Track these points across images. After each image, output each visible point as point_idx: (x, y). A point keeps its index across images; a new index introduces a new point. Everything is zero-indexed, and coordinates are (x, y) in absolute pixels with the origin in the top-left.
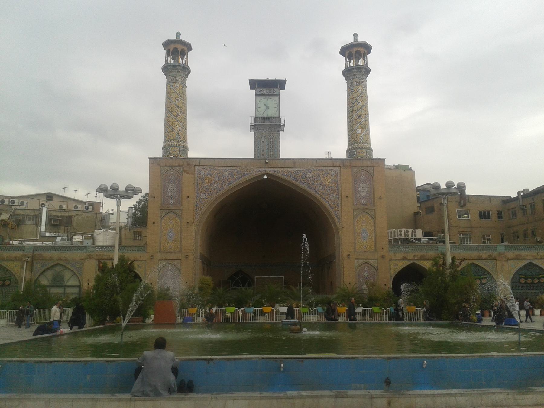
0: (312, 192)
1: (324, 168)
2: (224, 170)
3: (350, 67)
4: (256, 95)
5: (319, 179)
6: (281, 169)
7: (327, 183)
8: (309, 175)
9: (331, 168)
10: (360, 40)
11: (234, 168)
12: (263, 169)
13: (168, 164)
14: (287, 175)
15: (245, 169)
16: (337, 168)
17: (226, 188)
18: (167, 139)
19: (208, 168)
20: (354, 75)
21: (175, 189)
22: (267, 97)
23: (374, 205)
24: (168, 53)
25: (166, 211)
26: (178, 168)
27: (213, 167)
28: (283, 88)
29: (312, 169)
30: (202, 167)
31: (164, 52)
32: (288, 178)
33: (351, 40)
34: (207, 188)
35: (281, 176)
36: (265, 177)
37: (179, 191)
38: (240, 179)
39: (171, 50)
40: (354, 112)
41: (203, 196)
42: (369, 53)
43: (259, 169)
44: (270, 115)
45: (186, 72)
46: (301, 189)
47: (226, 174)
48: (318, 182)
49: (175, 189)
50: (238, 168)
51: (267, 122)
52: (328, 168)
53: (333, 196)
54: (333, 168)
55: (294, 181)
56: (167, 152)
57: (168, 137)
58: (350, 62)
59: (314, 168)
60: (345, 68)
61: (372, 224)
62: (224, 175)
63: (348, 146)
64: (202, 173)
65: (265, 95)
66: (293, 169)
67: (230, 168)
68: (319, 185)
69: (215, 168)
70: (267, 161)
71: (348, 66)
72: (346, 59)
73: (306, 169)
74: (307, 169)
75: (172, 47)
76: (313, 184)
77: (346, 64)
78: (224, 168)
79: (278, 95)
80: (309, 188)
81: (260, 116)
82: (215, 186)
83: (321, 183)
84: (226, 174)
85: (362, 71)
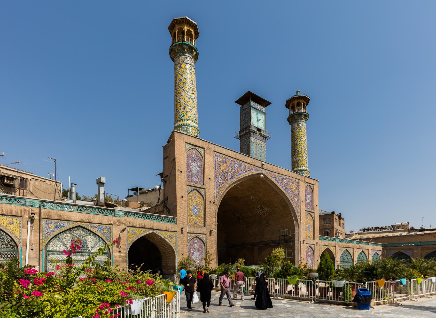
6: (270, 172)
7: (293, 190)
11: (241, 162)
12: (260, 169)
15: (249, 165)
17: (237, 178)
19: (224, 156)
23: (313, 209)
25: (191, 187)
32: (274, 180)
36: (262, 176)
37: (203, 171)
41: (220, 181)
43: (257, 168)
47: (236, 166)
50: (244, 163)
53: (296, 200)
54: (296, 180)
61: (312, 222)
64: (220, 160)
67: (239, 161)
69: (229, 158)
70: (264, 163)
78: (235, 160)
84: (236, 166)
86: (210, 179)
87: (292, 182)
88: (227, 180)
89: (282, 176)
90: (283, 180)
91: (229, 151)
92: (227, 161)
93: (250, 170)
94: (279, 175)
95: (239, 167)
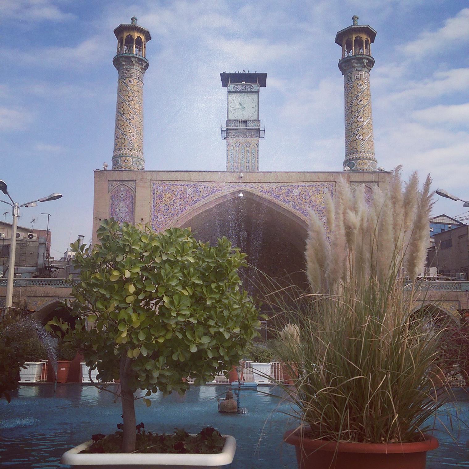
0: (299, 214)
1: (315, 184)
2: (187, 185)
3: (348, 57)
4: (230, 92)
5: (307, 197)
6: (260, 185)
7: (318, 203)
8: (296, 192)
9: (324, 183)
10: (362, 22)
13: (118, 179)
14: (266, 192)
15: (214, 184)
16: (331, 183)
18: (117, 147)
19: (168, 183)
20: (354, 67)
21: (127, 210)
22: (243, 95)
24: (121, 41)
26: (130, 184)
27: (173, 182)
28: (263, 84)
29: (298, 184)
30: (160, 182)
31: (115, 41)
32: (268, 196)
33: (349, 24)
34: (166, 208)
35: (260, 194)
37: (132, 212)
38: (208, 197)
39: (125, 37)
40: (354, 114)
42: (372, 41)
44: (245, 118)
45: (142, 65)
46: (285, 210)
48: (307, 201)
49: (127, 210)
50: (205, 184)
51: (243, 126)
52: (319, 184)
54: (326, 183)
55: (275, 200)
56: (117, 163)
57: (118, 146)
58: (348, 52)
59: (302, 184)
60: (343, 59)
62: (188, 192)
63: (346, 156)
64: (160, 189)
65: (240, 92)
66: (275, 184)
67: (194, 183)
68: (308, 205)
70: (242, 174)
71: (346, 56)
72: (343, 49)
73: (291, 184)
74: (293, 184)
75: (125, 35)
76: (300, 204)
77: (343, 54)
79: (257, 92)
80: (295, 208)
81: (233, 118)
82: (177, 206)
83: (310, 202)
84: (189, 191)
85: (363, 63)
86: (142, 219)
87: (314, 189)
88: (173, 214)
89: (286, 184)
90: (289, 191)
91: (177, 173)
92: (173, 188)
93: (217, 191)
94: (280, 185)
95: (194, 191)
